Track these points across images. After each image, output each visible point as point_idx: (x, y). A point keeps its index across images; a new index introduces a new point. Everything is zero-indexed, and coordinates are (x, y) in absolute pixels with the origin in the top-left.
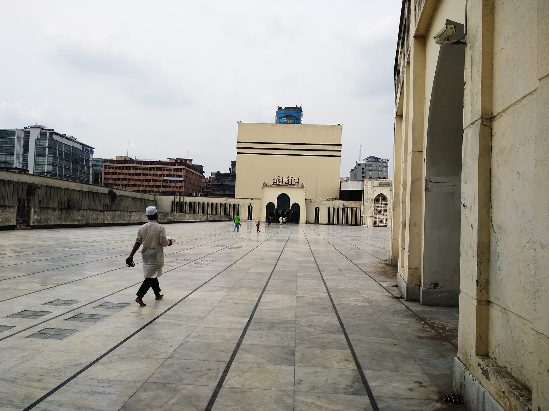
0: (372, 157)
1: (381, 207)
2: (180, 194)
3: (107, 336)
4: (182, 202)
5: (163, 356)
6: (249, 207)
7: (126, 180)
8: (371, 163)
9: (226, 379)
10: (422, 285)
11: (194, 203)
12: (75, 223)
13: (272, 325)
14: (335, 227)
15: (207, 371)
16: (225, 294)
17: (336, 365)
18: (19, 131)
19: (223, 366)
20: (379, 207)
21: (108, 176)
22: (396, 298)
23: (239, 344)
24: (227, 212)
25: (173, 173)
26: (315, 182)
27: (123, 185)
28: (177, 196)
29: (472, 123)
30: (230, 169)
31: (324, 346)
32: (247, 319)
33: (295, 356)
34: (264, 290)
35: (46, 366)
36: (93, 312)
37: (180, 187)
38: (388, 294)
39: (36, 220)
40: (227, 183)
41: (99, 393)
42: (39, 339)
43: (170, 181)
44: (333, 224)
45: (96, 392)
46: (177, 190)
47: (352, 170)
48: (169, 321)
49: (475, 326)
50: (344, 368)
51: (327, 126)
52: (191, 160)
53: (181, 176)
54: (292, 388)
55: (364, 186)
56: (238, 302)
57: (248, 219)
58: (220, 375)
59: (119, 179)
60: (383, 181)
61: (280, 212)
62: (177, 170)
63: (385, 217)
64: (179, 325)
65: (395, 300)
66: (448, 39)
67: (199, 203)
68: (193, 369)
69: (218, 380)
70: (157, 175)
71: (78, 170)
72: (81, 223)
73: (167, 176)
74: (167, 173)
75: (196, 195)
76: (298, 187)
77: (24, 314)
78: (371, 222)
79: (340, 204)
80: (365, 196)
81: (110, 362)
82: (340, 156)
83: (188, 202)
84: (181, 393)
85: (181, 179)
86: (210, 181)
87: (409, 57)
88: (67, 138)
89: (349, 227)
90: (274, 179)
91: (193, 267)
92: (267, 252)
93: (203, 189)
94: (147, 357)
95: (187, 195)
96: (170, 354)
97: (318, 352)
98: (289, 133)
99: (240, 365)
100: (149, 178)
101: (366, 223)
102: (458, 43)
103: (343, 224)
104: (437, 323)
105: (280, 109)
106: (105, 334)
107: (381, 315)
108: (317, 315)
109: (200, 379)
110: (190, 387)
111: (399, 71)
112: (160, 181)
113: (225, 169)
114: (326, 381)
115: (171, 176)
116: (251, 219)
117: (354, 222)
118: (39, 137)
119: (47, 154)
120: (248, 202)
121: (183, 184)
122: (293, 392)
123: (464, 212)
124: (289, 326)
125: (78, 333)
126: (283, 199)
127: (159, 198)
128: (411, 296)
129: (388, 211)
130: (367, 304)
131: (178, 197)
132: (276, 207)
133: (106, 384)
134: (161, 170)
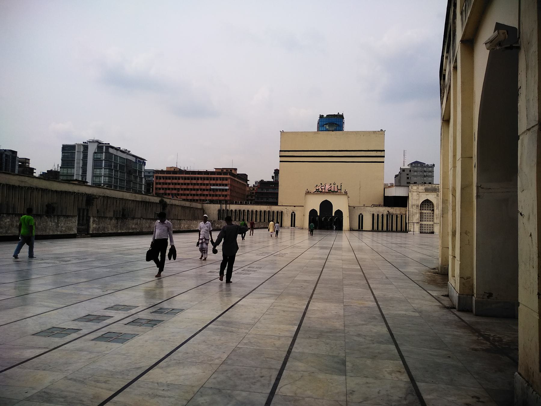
0: (417, 162)
1: (428, 213)
2: (226, 203)
3: (164, 340)
4: (227, 210)
5: (217, 361)
6: (292, 214)
7: (175, 189)
8: (416, 168)
9: (279, 387)
10: (475, 295)
11: (240, 211)
12: (130, 231)
13: (321, 334)
14: (380, 234)
15: (260, 378)
16: (273, 301)
17: (388, 376)
18: (79, 145)
19: (275, 374)
20: (425, 213)
21: (159, 186)
22: (447, 308)
23: (289, 352)
25: (219, 182)
26: (358, 189)
27: (172, 194)
29: (529, 130)
30: (273, 177)
31: (375, 356)
32: (296, 327)
33: (345, 365)
34: (311, 298)
35: (111, 369)
36: (151, 317)
37: (226, 196)
38: (438, 304)
39: (95, 229)
40: (271, 191)
41: (159, 396)
42: (103, 343)
43: (217, 190)
44: (378, 231)
45: (157, 395)
46: (223, 198)
47: (396, 176)
48: (221, 327)
49: (538, 341)
50: (396, 379)
51: (369, 132)
52: (236, 169)
53: (226, 185)
54: (345, 398)
55: (409, 191)
56: (286, 309)
57: (292, 226)
58: (273, 382)
59: (169, 189)
60: (429, 186)
61: (323, 219)
62: (223, 179)
63: (431, 223)
64: (230, 332)
65: (446, 310)
66: (500, 44)
67: (244, 211)
68: (246, 376)
69: (271, 387)
70: (204, 184)
72: (135, 231)
73: (214, 185)
74: (213, 182)
75: (241, 204)
76: (341, 194)
77: (89, 318)
78: (417, 228)
79: (384, 210)
80: (411, 202)
81: (168, 366)
82: (383, 162)
83: (234, 210)
84: (236, 399)
85: (227, 188)
86: (254, 189)
87: (456, 61)
88: (122, 151)
89: (394, 234)
91: (241, 273)
92: (312, 259)
93: (247, 197)
94: (201, 363)
95: (232, 203)
96: (223, 360)
97: (369, 362)
98: (331, 140)
99: (292, 373)
100: (196, 187)
101: (412, 230)
102: (511, 48)
103: (387, 231)
104: (492, 335)
105: (321, 117)
106: (162, 338)
107: (433, 326)
108: (366, 324)
109: (253, 386)
110: (244, 394)
111: (444, 75)
112: (207, 190)
113: (268, 178)
114: (379, 393)
115: (217, 185)
116: (294, 226)
117: (399, 228)
118: (96, 151)
119: (103, 166)
120: (291, 209)
121: (228, 193)
122: (345, 403)
123: (521, 221)
124: (338, 335)
125: (137, 338)
126: (326, 206)
127: (207, 206)
128: (463, 306)
129: (435, 217)
130: (417, 314)
131: (224, 206)
132: (319, 214)
133: (166, 388)
134: (208, 179)
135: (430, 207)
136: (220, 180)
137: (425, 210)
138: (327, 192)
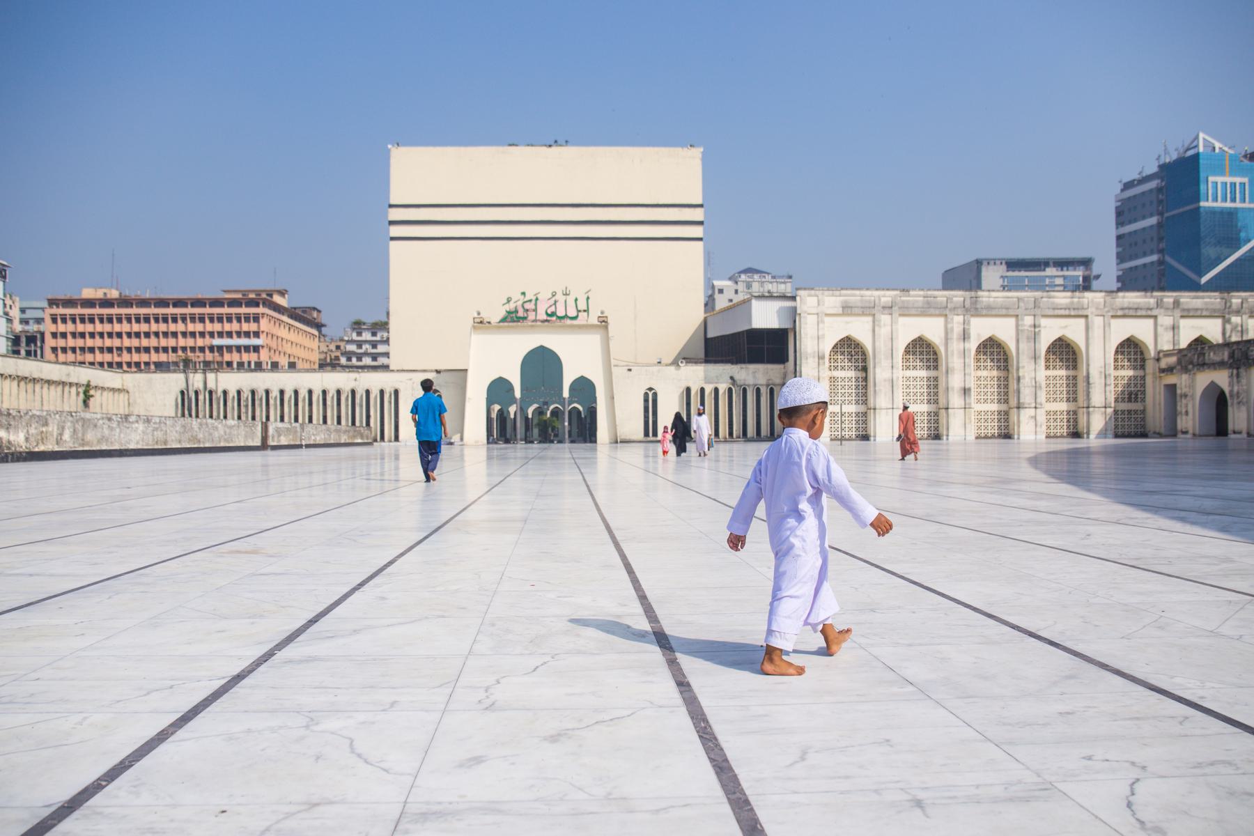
4: (211, 393)
20: (843, 379)
28: (196, 371)
55: (794, 314)
63: (862, 408)
90: (509, 300)
126: (542, 365)
132: (518, 394)
135: (857, 360)
138: (543, 321)
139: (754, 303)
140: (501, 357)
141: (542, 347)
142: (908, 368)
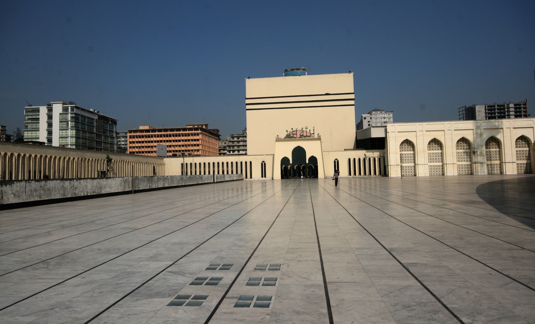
20: (405, 154)
24: (239, 172)
52: (206, 125)
57: (262, 177)
71: (80, 138)
93: (220, 150)
112: (180, 146)
126: (299, 152)
132: (291, 162)
136: (192, 135)
137: (405, 151)
139: (372, 128)
140: (286, 150)
141: (299, 147)
142: (430, 150)
